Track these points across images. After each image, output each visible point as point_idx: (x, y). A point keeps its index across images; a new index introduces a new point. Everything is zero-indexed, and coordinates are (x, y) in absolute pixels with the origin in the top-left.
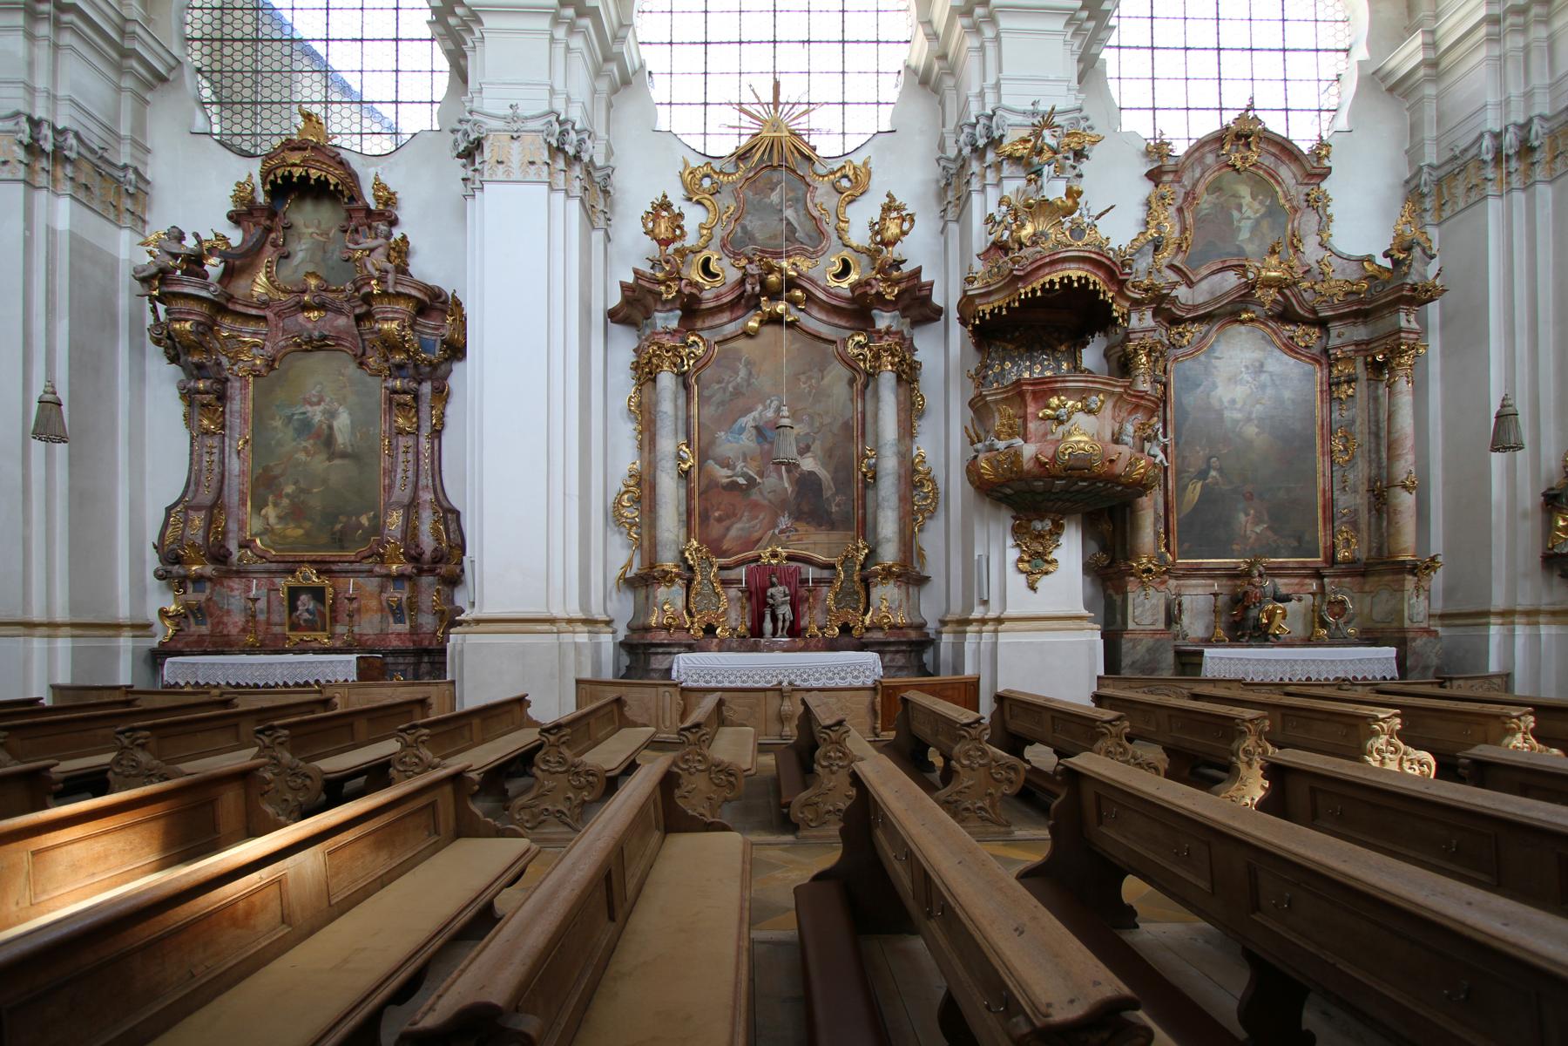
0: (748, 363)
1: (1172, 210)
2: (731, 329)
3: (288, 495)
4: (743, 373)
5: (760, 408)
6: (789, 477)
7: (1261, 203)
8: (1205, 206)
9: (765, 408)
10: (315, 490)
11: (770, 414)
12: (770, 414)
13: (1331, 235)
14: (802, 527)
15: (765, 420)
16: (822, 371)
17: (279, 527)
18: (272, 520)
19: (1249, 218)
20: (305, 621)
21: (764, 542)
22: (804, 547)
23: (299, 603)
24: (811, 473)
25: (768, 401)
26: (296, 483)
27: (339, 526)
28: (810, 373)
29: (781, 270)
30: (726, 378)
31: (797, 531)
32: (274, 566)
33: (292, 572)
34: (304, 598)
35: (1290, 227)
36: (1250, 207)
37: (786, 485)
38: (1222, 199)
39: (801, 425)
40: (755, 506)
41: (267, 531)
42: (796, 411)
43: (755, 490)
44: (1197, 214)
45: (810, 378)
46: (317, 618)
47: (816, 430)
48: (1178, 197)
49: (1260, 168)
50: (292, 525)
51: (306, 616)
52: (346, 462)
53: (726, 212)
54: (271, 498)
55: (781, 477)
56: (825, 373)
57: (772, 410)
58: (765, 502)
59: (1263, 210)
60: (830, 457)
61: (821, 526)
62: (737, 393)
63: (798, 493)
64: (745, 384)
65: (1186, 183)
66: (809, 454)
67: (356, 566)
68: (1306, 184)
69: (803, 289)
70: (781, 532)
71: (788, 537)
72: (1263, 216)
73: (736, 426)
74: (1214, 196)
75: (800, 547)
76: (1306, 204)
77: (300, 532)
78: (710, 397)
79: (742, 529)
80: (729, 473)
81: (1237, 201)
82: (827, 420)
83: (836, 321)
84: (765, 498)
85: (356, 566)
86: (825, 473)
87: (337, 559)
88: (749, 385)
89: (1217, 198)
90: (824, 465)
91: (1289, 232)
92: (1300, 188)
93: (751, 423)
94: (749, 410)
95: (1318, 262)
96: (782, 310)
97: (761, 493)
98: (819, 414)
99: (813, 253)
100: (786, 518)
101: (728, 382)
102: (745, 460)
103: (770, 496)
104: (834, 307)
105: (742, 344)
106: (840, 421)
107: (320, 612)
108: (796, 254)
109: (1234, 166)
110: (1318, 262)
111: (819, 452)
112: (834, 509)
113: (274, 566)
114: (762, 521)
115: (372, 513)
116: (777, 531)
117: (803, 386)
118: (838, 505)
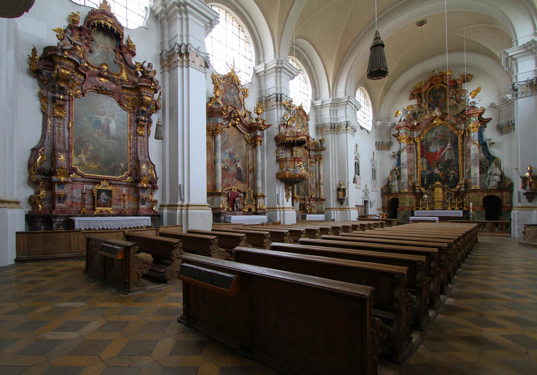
0: (227, 135)
3: (90, 151)
4: (226, 137)
10: (102, 150)
14: (238, 182)
17: (86, 163)
18: (84, 160)
20: (103, 203)
23: (101, 196)
24: (240, 168)
26: (94, 146)
27: (112, 166)
32: (88, 180)
33: (99, 183)
34: (103, 194)
40: (229, 175)
41: (81, 164)
43: (229, 171)
46: (108, 202)
50: (92, 163)
51: (104, 201)
52: (115, 141)
54: (83, 150)
58: (231, 174)
63: (237, 173)
67: (119, 182)
70: (234, 183)
73: (225, 152)
77: (96, 166)
79: (227, 181)
80: (224, 165)
82: (242, 154)
83: (244, 128)
85: (119, 182)
87: (113, 179)
88: (228, 141)
90: (242, 166)
93: (228, 152)
94: (228, 148)
102: (227, 162)
104: (245, 125)
107: (109, 200)
112: (244, 178)
113: (88, 180)
115: (125, 163)
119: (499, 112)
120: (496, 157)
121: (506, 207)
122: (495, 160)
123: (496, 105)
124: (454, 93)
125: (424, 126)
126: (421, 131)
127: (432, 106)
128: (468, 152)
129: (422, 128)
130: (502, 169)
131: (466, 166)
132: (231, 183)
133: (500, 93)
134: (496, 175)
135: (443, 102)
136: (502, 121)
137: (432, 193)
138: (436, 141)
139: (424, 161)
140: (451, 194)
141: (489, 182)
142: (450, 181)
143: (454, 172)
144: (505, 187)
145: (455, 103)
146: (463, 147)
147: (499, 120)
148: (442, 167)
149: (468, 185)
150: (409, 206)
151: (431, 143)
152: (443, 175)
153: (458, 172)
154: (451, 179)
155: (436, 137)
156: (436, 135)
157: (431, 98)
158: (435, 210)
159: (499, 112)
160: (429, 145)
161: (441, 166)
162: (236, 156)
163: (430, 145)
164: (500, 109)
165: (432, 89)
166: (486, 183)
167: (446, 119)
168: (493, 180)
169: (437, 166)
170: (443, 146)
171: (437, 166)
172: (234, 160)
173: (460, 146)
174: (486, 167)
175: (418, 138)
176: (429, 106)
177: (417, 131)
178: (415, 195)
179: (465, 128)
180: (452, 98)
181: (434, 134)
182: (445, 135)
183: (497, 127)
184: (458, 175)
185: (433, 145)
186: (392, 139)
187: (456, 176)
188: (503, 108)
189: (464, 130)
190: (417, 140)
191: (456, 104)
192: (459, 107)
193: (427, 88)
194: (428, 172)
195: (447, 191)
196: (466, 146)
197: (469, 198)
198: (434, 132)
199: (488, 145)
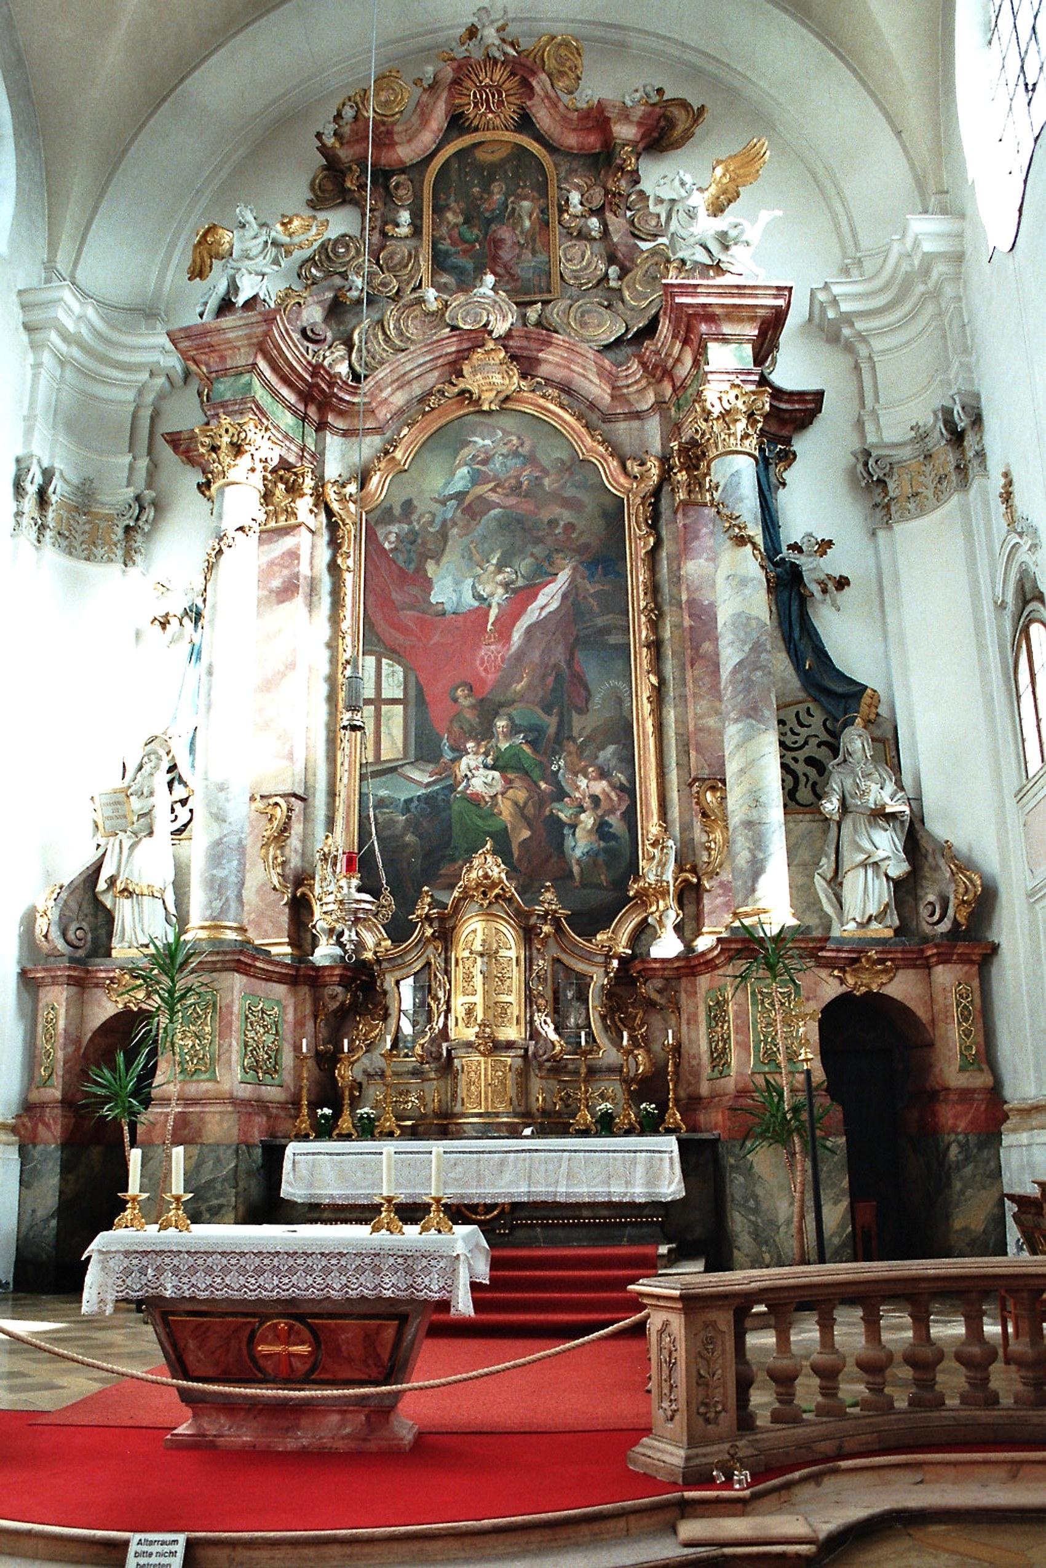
119: (857, 368)
120: (866, 687)
121: (965, 1095)
122: (864, 708)
123: (845, 307)
124: (596, 203)
125: (399, 399)
126: (376, 441)
127: (458, 271)
128: (687, 622)
129: (383, 414)
130: (907, 779)
131: (684, 748)
133: (851, 251)
134: (880, 816)
135: (527, 254)
136: (879, 428)
137: (438, 963)
138: (479, 530)
139: (384, 685)
140: (582, 984)
141: (836, 882)
142: (576, 869)
143: (600, 787)
144: (945, 927)
145: (602, 266)
146: (654, 589)
147: (860, 424)
148: (519, 739)
149: (699, 901)
150: (244, 1092)
151: (443, 536)
152: (520, 809)
153: (628, 791)
154: (578, 853)
155: (480, 490)
156: (477, 478)
157: (449, 216)
158: (458, 1135)
159: (857, 368)
160: (424, 557)
161: (514, 729)
163: (437, 556)
164: (863, 351)
165: (459, 154)
166: (820, 883)
167: (544, 370)
168: (864, 865)
169: (485, 733)
170: (525, 565)
171: (485, 733)
173: (638, 577)
174: (810, 761)
175: (352, 488)
176: (439, 262)
177: (346, 434)
178: (305, 990)
179: (665, 441)
180: (583, 235)
181: (465, 470)
182: (537, 482)
183: (852, 472)
184: (630, 817)
185: (452, 557)
186: (163, 477)
187: (614, 820)
188: (877, 344)
189: (664, 460)
190: (343, 499)
191: (606, 277)
192: (626, 293)
193: (427, 139)
194: (416, 775)
195: (554, 951)
196: (677, 579)
197: (717, 1014)
198: (466, 453)
199: (815, 589)
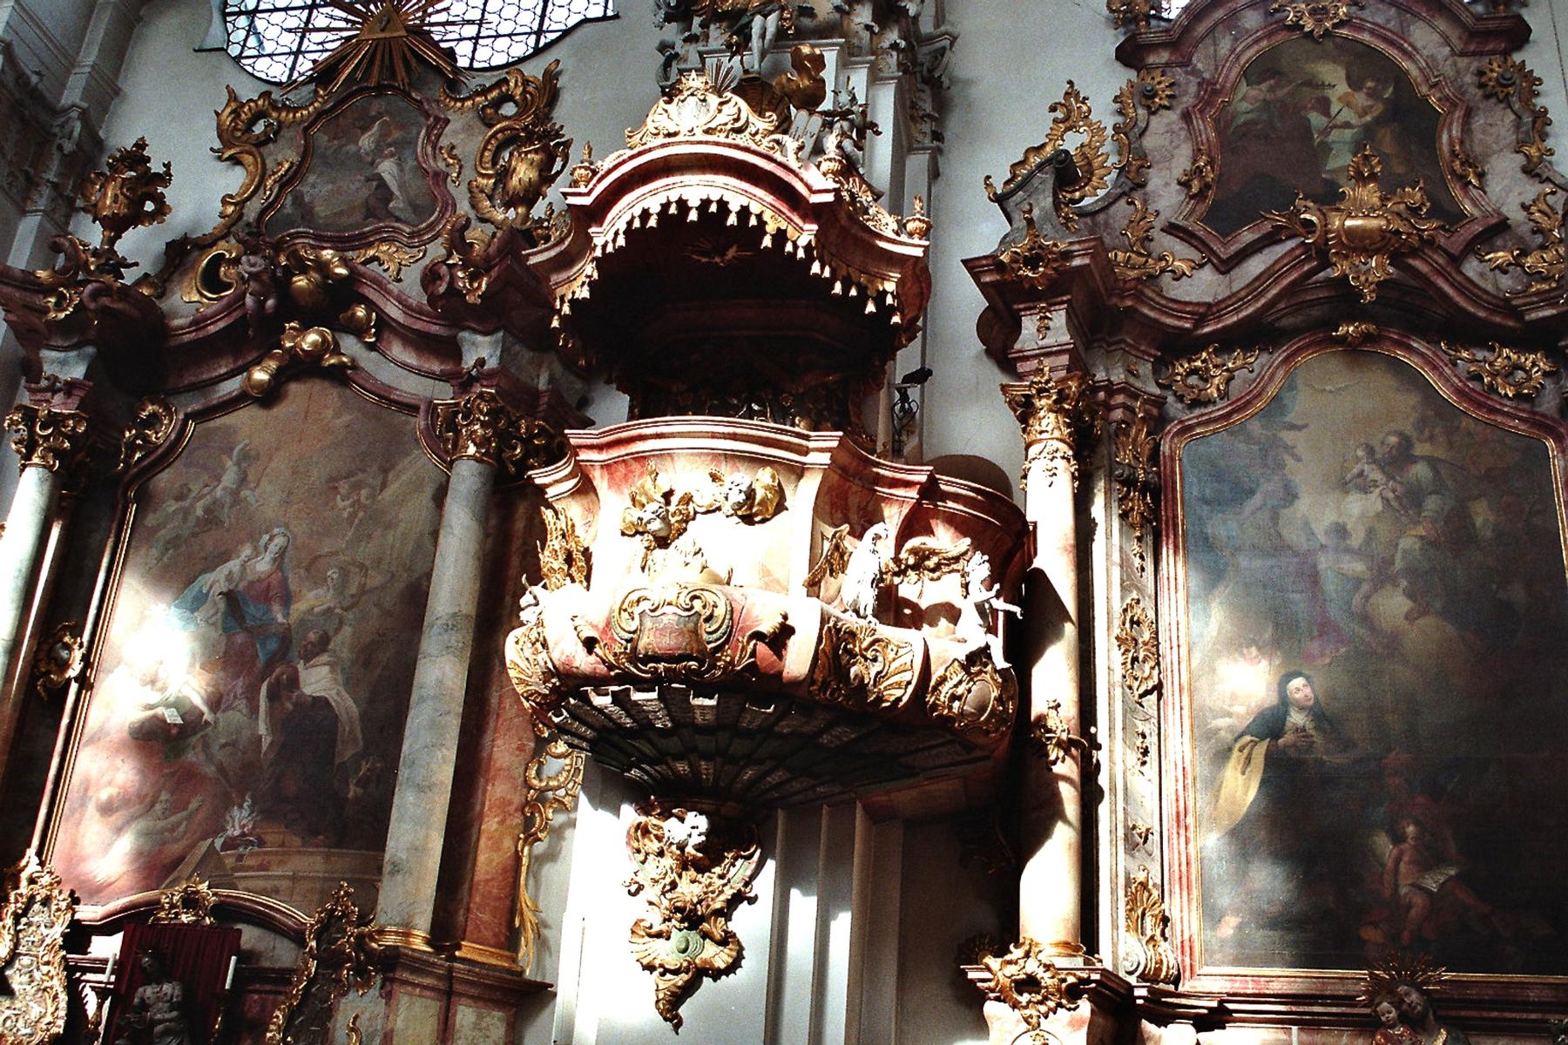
1: (1173, 116)
2: (231, 386)
4: (229, 478)
5: (247, 551)
6: (271, 712)
7: (1372, 94)
8: (1245, 106)
9: (257, 552)
11: (263, 565)
12: (263, 565)
13: (1551, 152)
15: (250, 578)
16: (385, 471)
19: (1347, 125)
21: (185, 869)
22: (269, 884)
24: (321, 703)
25: (266, 537)
28: (360, 476)
29: (323, 267)
30: (195, 488)
31: (261, 843)
35: (1445, 138)
36: (1348, 105)
37: (262, 729)
38: (1280, 93)
39: (321, 591)
42: (317, 558)
44: (1228, 124)
45: (357, 487)
47: (346, 604)
48: (1186, 93)
49: (1361, 29)
53: (274, 173)
55: (254, 710)
56: (391, 476)
57: (268, 557)
58: (210, 770)
59: (1379, 109)
60: (367, 664)
61: (314, 833)
62: (212, 518)
64: (228, 500)
65: (1200, 66)
66: (325, 658)
68: (1474, 54)
69: (371, 305)
70: (230, 844)
71: (240, 857)
72: (1378, 121)
74: (1264, 86)
75: (261, 884)
76: (1480, 93)
78: (156, 529)
81: (1318, 93)
82: (375, 580)
84: (210, 758)
86: (350, 703)
89: (1271, 89)
90: (350, 684)
91: (1446, 148)
92: (1462, 62)
93: (223, 586)
94: (224, 557)
95: (1525, 207)
96: (314, 344)
97: (206, 747)
98: (362, 567)
99: (412, 235)
100: (245, 813)
101: (198, 498)
103: (220, 755)
105: (245, 419)
106: (400, 585)
108: (383, 240)
109: (1297, 27)
110: (1525, 207)
111: (345, 654)
112: (353, 791)
114: (190, 817)
116: (218, 843)
117: (341, 504)
118: (363, 783)
132: (192, 846)
162: (299, 607)
172: (273, 645)
